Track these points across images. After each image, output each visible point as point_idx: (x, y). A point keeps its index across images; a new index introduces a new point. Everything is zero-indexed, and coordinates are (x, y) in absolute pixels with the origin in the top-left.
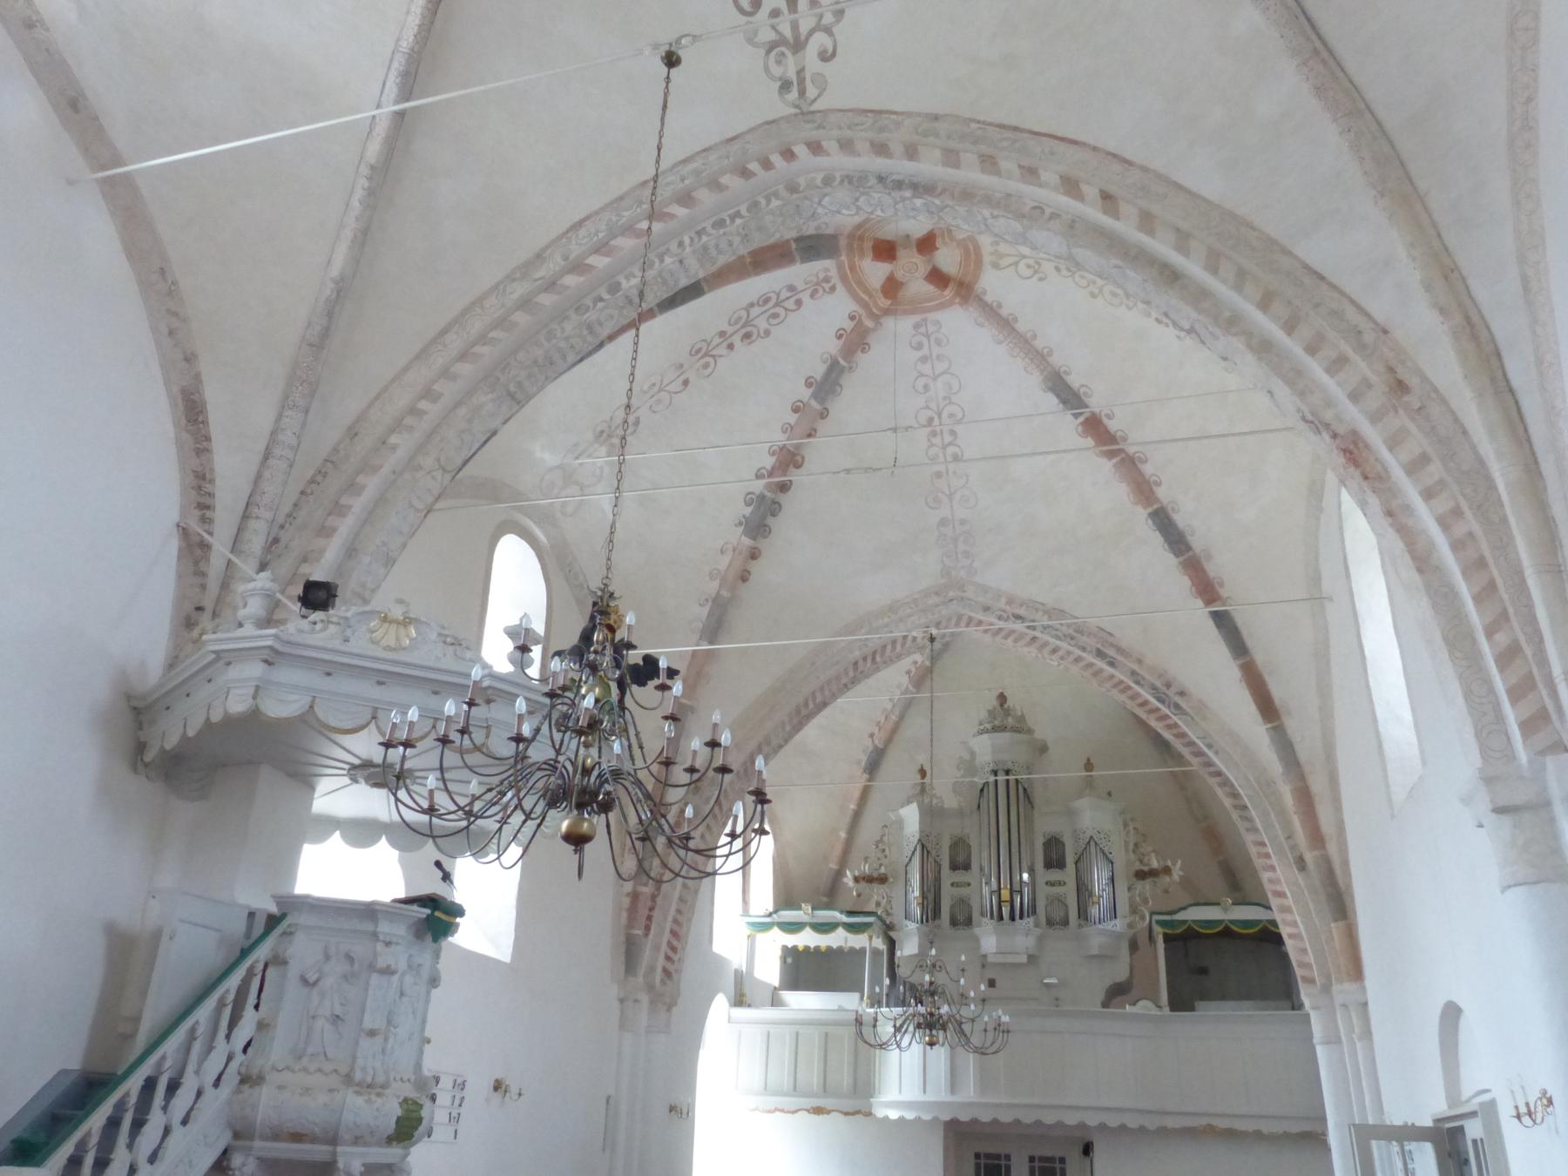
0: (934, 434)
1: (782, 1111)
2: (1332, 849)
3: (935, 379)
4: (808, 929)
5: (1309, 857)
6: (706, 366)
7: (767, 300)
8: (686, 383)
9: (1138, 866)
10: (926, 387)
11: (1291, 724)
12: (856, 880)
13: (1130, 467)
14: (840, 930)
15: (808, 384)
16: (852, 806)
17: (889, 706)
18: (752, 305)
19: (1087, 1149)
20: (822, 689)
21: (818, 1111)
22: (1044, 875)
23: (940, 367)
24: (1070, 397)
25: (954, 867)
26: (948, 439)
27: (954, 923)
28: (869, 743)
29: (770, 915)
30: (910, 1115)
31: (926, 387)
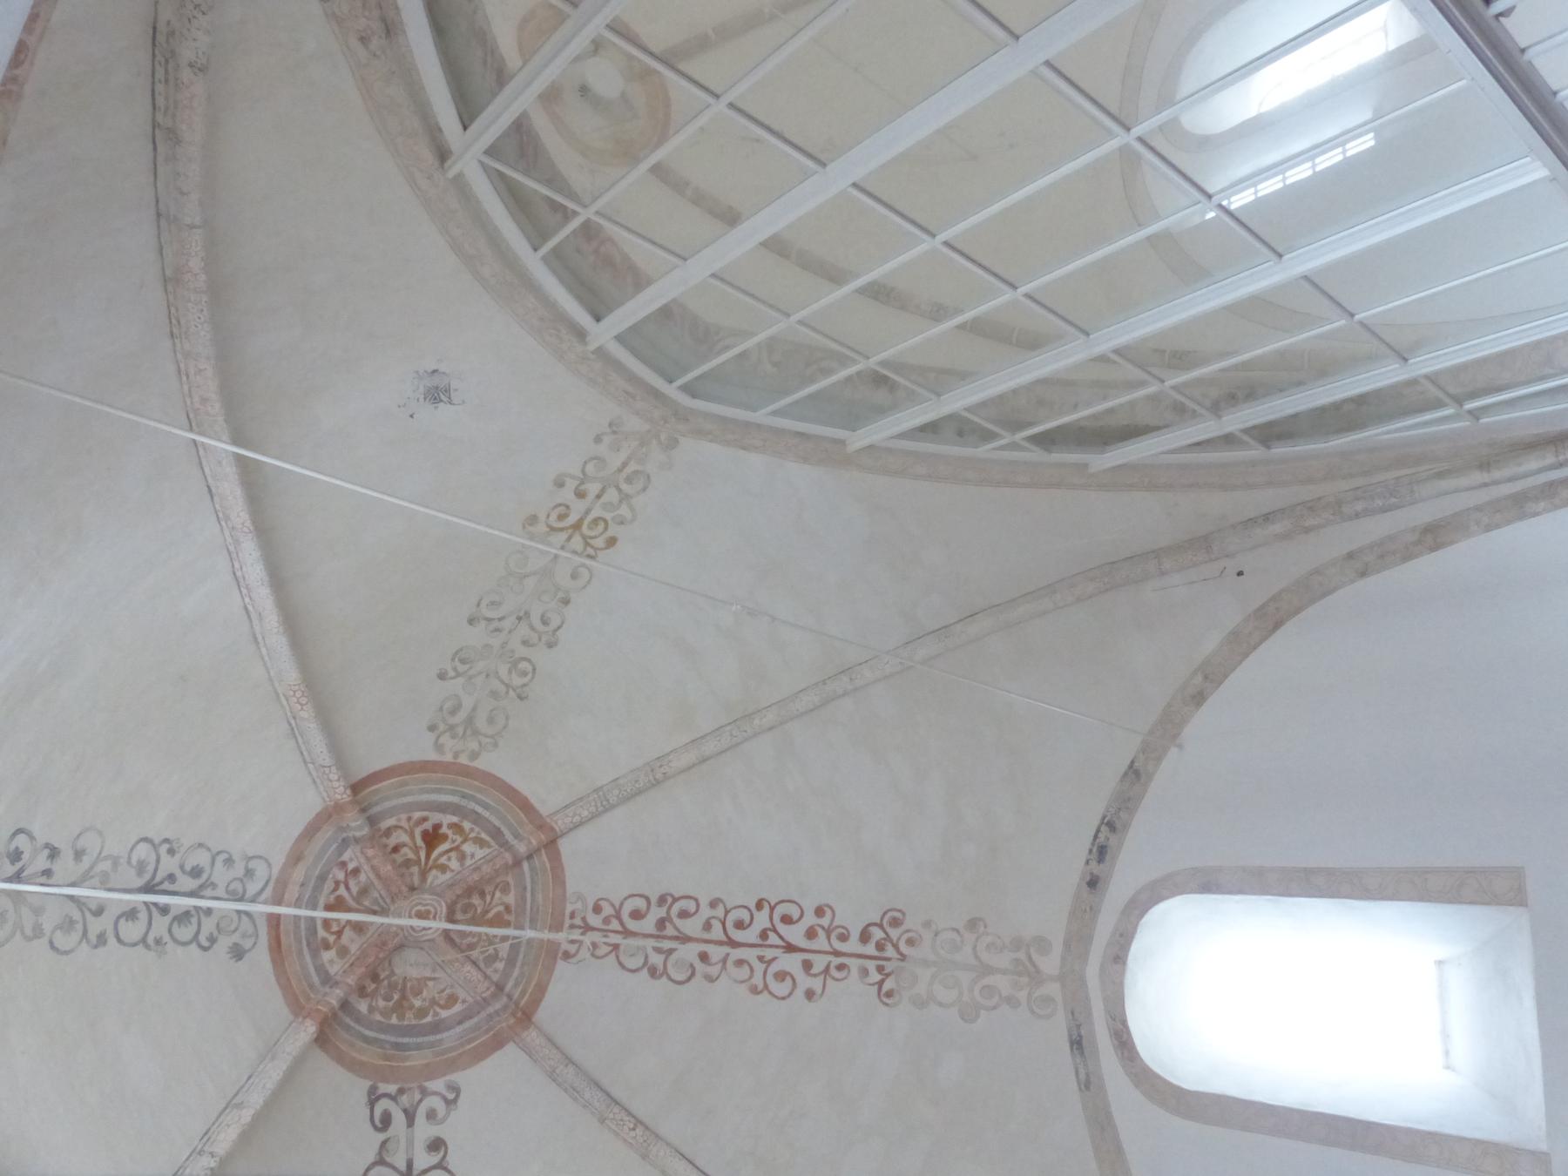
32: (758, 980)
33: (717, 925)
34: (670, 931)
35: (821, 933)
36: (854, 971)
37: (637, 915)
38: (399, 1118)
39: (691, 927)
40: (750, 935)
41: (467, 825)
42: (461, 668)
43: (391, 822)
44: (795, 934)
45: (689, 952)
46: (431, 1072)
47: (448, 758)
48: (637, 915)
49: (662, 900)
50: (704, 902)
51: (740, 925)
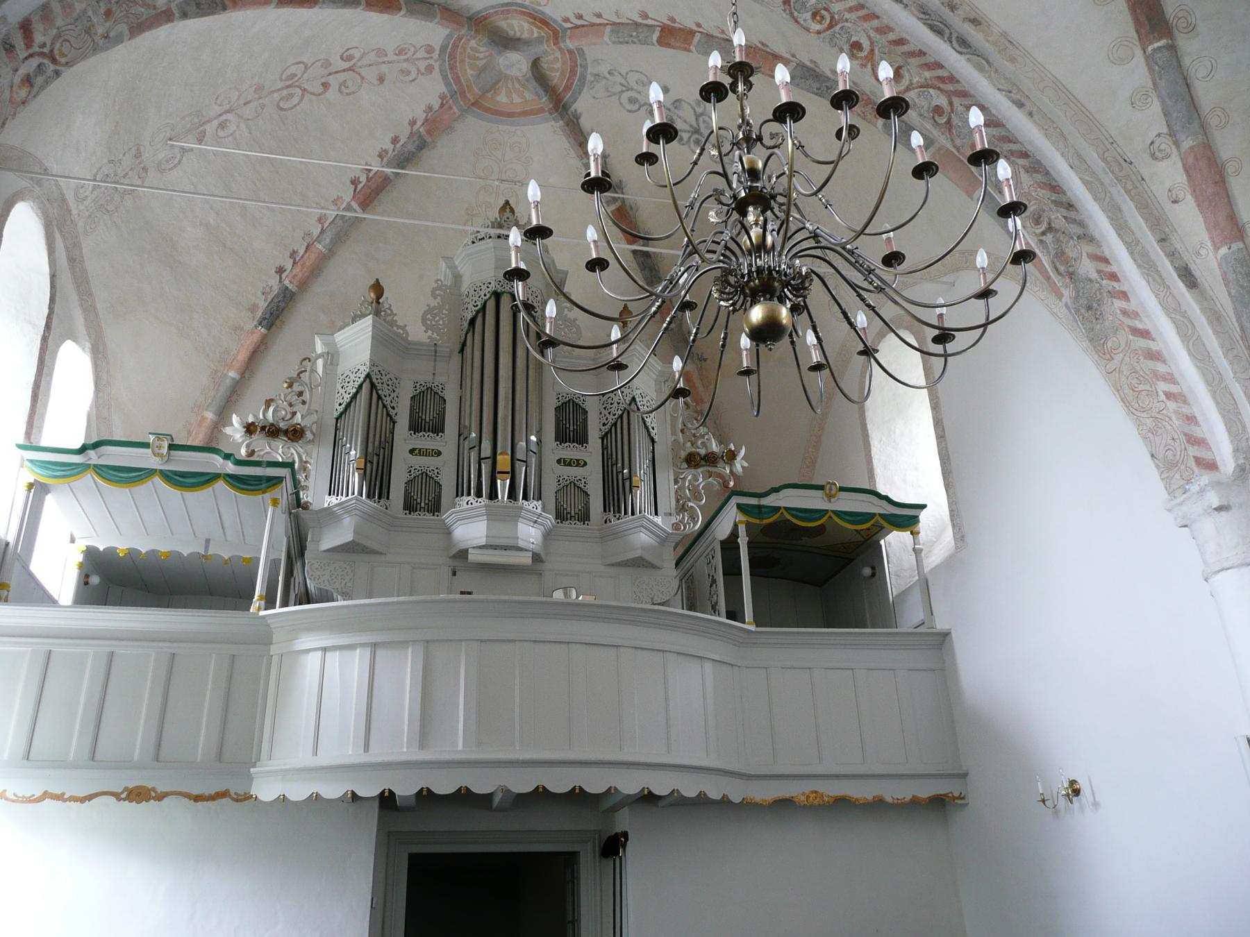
1: (59, 797)
4: (157, 479)
9: (689, 448)
12: (250, 429)
14: (220, 485)
16: (233, 374)
17: (316, 231)
19: (613, 846)
21: (138, 795)
22: (554, 451)
25: (416, 426)
27: (410, 506)
28: (274, 282)
29: (83, 450)
30: (333, 790)
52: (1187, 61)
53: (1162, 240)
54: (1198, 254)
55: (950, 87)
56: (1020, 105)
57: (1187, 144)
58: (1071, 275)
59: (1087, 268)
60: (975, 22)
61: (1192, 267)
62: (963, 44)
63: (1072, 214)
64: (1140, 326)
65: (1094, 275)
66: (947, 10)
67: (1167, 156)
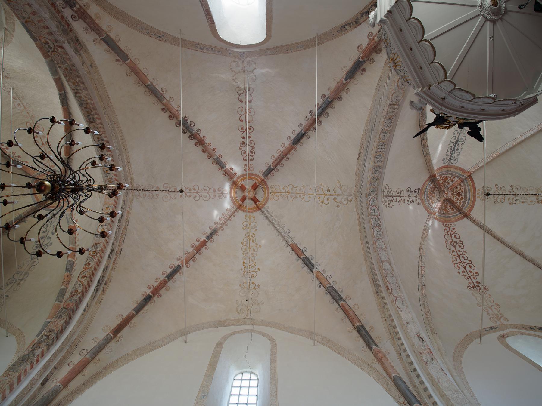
0: (190, 190)
2: (64, 393)
3: (208, 193)
5: (52, 385)
6: (242, 129)
7: (252, 153)
8: (242, 121)
10: (205, 190)
11: (113, 343)
13: (190, 258)
15: (220, 155)
18: (253, 148)
20: (101, 123)
23: (212, 196)
24: (210, 237)
26: (188, 194)
31: (205, 190)
32: (455, 262)
33: (461, 253)
34: (455, 244)
35: (472, 274)
36: (469, 281)
37: (455, 237)
38: (415, 194)
39: (458, 248)
40: (463, 260)
41: (463, 200)
42: (499, 189)
43: (462, 185)
44: (468, 268)
45: (453, 249)
46: (422, 200)
47: (477, 193)
48: (455, 237)
49: (461, 241)
50: (464, 250)
51: (463, 257)
52: (109, 345)
53: (55, 368)
54: (54, 380)
55: (84, 291)
56: (84, 311)
57: (87, 357)
58: (34, 349)
59: (38, 352)
60: (103, 291)
61: (49, 381)
62: (97, 290)
63: (55, 340)
64: (22, 377)
65: (36, 355)
66: (104, 282)
67: (81, 355)
